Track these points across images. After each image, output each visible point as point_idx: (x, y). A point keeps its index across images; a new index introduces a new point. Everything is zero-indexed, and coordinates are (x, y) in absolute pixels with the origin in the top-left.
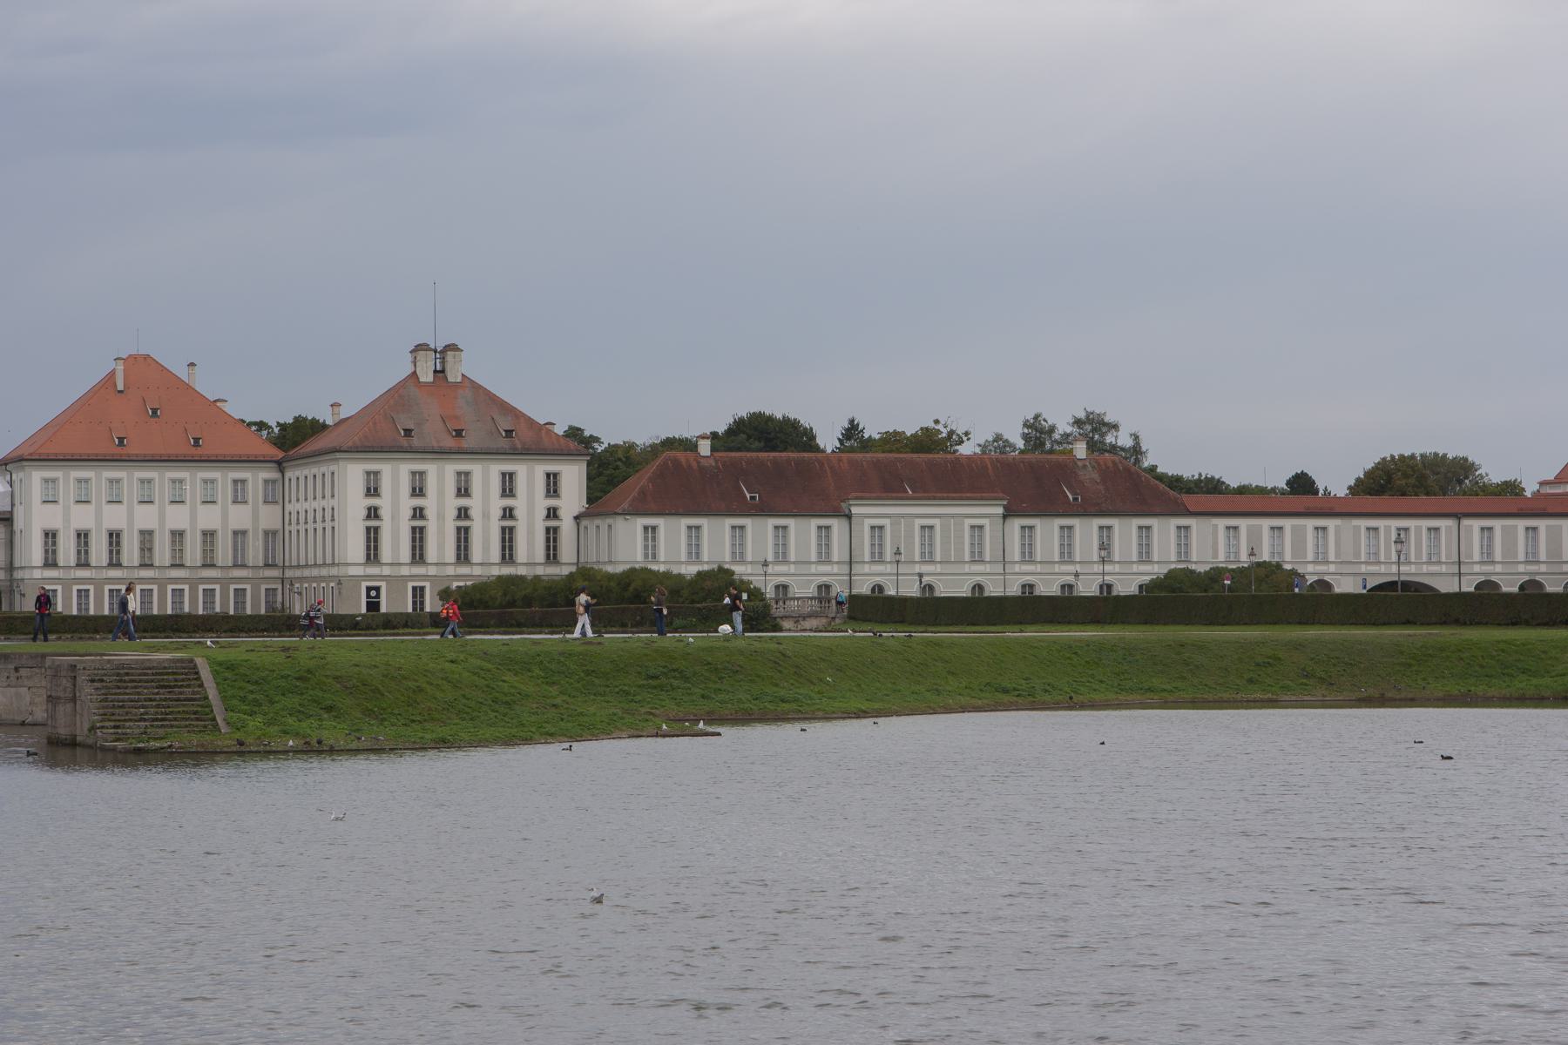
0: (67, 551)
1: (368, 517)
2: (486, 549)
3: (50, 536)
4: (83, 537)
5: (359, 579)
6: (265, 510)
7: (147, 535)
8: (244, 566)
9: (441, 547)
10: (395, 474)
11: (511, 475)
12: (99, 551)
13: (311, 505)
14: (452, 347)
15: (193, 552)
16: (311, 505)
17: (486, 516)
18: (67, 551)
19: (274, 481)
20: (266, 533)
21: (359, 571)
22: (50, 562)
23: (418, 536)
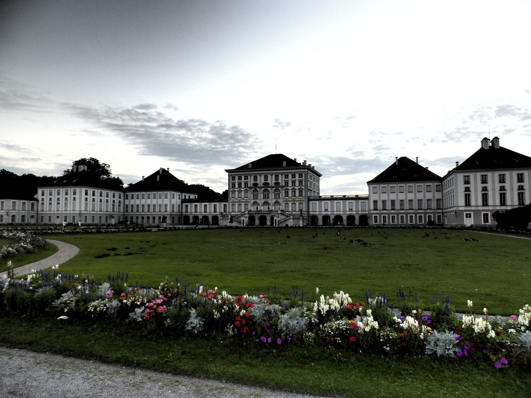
0: (380, 206)
1: (466, 191)
2: (512, 200)
3: (375, 202)
4: (384, 202)
5: (462, 211)
6: (436, 193)
7: (402, 201)
8: (431, 209)
9: (494, 200)
10: (475, 177)
11: (522, 174)
12: (389, 206)
13: (449, 189)
14: (496, 138)
15: (415, 206)
16: (449, 189)
17: (512, 189)
18: (380, 206)
19: (439, 185)
20: (437, 200)
21: (463, 209)
22: (375, 209)
23: (485, 197)
